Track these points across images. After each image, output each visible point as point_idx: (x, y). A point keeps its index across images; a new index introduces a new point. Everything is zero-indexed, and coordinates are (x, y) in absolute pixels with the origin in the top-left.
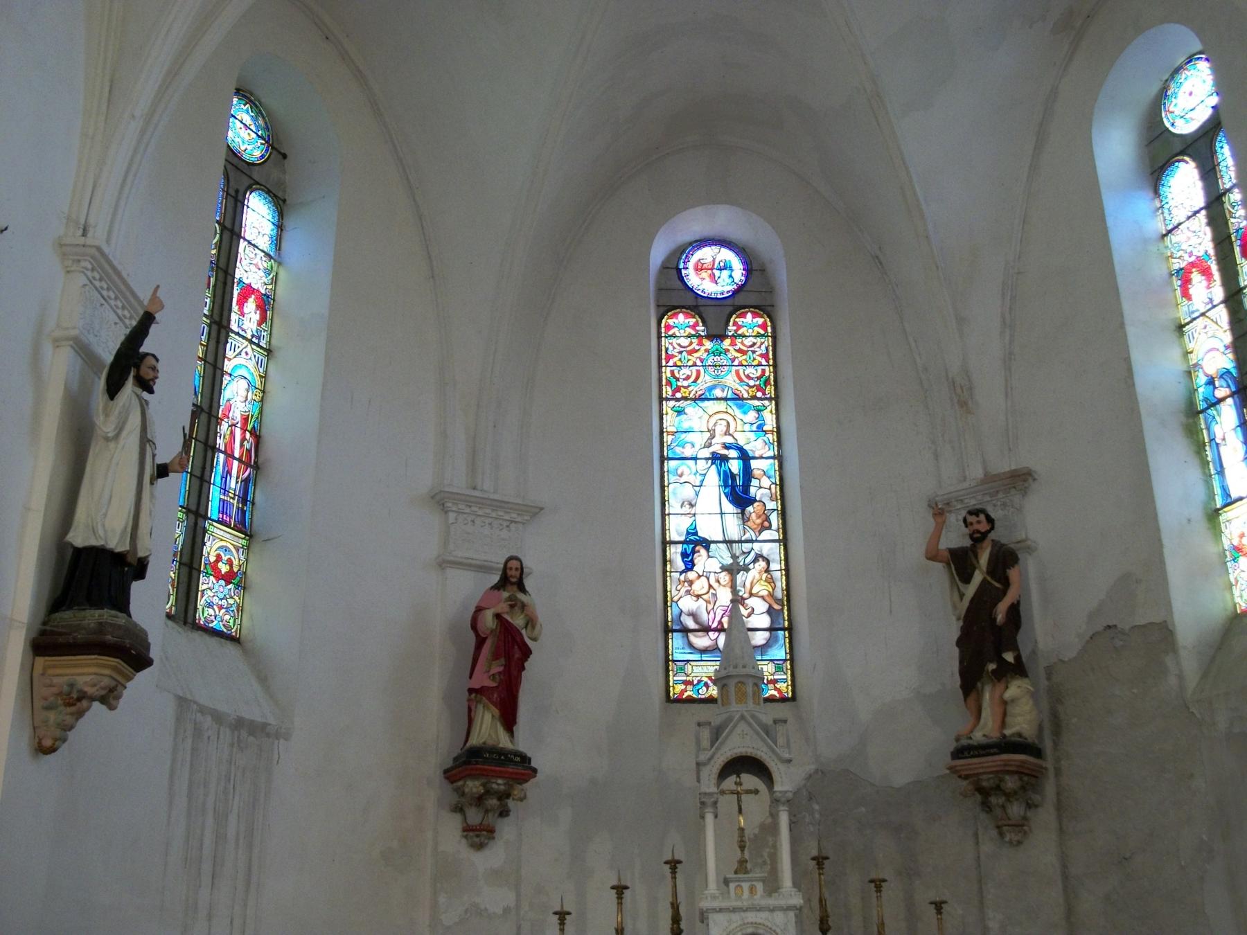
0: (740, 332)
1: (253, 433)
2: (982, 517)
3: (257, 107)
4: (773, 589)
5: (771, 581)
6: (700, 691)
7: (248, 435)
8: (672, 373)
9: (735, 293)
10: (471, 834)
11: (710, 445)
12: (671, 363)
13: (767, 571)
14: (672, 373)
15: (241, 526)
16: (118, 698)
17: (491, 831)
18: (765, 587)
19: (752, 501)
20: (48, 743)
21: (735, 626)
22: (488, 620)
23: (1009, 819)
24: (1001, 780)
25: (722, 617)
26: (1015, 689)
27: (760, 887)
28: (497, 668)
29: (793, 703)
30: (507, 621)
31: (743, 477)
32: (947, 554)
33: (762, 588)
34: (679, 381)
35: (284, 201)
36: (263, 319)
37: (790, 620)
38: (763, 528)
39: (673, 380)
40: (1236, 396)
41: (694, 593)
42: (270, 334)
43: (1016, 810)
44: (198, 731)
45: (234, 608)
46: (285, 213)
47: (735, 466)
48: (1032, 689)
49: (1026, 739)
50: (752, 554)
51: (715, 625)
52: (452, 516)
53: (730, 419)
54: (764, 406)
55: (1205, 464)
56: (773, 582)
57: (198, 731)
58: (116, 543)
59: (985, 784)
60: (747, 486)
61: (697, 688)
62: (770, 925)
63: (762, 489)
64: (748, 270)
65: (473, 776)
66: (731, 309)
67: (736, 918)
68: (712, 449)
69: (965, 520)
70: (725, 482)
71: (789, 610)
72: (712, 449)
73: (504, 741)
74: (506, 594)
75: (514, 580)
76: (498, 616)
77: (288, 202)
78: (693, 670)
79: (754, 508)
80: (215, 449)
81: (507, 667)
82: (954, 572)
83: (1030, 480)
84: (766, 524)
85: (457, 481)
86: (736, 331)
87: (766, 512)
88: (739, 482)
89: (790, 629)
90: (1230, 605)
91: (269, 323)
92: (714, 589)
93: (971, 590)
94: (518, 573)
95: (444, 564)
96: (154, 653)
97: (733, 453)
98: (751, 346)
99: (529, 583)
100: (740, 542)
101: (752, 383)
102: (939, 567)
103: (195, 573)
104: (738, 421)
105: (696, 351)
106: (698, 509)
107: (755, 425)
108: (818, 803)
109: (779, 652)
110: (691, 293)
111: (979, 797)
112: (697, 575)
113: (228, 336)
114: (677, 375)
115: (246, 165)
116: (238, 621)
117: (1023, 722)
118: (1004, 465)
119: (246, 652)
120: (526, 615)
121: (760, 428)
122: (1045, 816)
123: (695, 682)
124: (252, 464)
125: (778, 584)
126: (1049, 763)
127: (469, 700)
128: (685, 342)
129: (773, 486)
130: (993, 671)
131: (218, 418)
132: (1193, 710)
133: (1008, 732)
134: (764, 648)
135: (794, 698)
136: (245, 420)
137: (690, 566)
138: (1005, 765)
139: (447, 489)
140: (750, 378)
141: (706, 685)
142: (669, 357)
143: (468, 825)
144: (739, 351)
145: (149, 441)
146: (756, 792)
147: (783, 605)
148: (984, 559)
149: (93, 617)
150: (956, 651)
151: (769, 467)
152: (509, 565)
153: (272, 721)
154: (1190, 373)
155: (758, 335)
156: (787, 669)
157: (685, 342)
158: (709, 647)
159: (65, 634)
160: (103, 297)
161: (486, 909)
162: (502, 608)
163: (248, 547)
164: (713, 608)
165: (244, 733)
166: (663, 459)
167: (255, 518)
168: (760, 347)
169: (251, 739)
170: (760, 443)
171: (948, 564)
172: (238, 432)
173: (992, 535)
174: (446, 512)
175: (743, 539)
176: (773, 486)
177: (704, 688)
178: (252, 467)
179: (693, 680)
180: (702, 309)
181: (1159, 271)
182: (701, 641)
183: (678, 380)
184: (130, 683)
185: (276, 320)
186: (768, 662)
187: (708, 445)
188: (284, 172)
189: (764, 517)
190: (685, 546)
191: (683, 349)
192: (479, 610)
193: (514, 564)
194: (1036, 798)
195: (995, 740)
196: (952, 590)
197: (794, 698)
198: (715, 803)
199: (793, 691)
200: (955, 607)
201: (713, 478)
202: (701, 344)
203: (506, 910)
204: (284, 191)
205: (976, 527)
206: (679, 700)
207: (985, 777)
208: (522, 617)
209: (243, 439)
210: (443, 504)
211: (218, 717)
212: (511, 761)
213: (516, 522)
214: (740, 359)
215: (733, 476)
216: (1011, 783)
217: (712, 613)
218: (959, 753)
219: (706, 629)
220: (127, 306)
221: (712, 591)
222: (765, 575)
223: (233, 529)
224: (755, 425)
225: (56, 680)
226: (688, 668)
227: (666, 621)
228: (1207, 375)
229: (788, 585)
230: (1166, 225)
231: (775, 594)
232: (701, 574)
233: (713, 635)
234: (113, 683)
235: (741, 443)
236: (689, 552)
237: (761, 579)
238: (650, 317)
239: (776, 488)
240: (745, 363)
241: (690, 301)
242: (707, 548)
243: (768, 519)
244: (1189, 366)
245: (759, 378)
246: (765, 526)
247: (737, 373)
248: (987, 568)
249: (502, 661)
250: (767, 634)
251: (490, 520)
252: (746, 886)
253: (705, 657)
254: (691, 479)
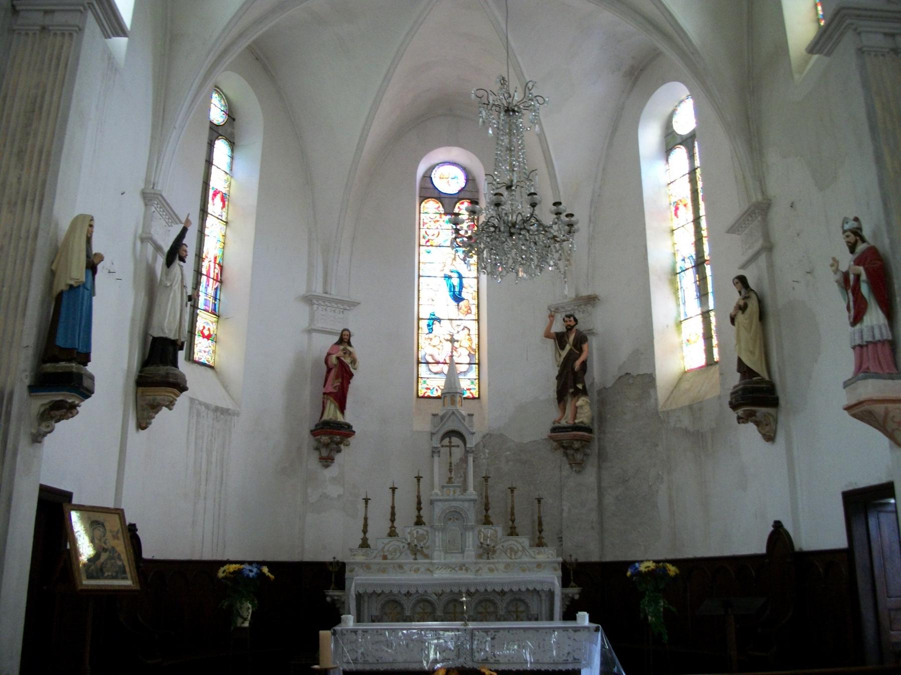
1: (219, 264)
2: (572, 319)
3: (221, 95)
4: (471, 344)
5: (470, 340)
7: (217, 266)
9: (460, 191)
10: (323, 460)
12: (426, 226)
15: (214, 312)
16: (173, 405)
17: (333, 459)
19: (463, 299)
20: (144, 425)
21: (452, 364)
22: (333, 360)
23: (575, 461)
24: (572, 443)
26: (581, 401)
27: (458, 490)
28: (338, 383)
29: (478, 400)
30: (342, 360)
32: (554, 335)
33: (466, 343)
35: (234, 143)
36: (224, 206)
37: (479, 360)
39: (426, 236)
40: (694, 268)
42: (227, 214)
43: (579, 457)
44: (198, 414)
45: (211, 352)
46: (235, 151)
47: (455, 281)
48: (589, 401)
49: (585, 424)
52: (315, 306)
55: (677, 299)
57: (198, 414)
58: (172, 336)
59: (565, 444)
60: (460, 292)
62: (462, 508)
63: (469, 293)
64: (467, 180)
65: (325, 434)
66: (456, 200)
67: (446, 503)
69: (564, 320)
70: (450, 289)
71: (479, 355)
73: (340, 418)
74: (342, 347)
75: (346, 340)
76: (338, 358)
77: (236, 144)
80: (201, 274)
81: (342, 383)
82: (557, 344)
83: (597, 301)
84: (469, 311)
85: (318, 290)
88: (457, 289)
89: (479, 364)
90: (683, 366)
91: (226, 207)
93: (564, 353)
95: (310, 331)
96: (188, 385)
97: (455, 275)
99: (352, 340)
102: (552, 341)
103: (193, 335)
105: (438, 221)
108: (487, 449)
109: (473, 374)
110: (437, 191)
111: (562, 450)
113: (207, 216)
115: (216, 127)
116: (213, 358)
117: (585, 416)
118: (585, 293)
119: (216, 372)
120: (352, 357)
122: (593, 460)
124: (219, 280)
126: (595, 435)
127: (323, 398)
128: (433, 216)
130: (572, 392)
131: (203, 258)
132: (660, 415)
133: (576, 421)
134: (465, 373)
135: (479, 398)
136: (215, 258)
137: (431, 331)
138: (575, 437)
139: (313, 294)
142: (424, 224)
143: (322, 456)
145: (185, 286)
146: (458, 446)
147: (476, 352)
148: (572, 338)
149: (163, 370)
150: (556, 381)
152: (344, 333)
153: (230, 407)
154: (674, 254)
157: (433, 216)
159: (151, 377)
160: (160, 215)
161: (330, 496)
162: (340, 354)
163: (218, 322)
165: (219, 414)
166: (419, 276)
167: (220, 307)
169: (222, 416)
171: (555, 340)
172: (212, 264)
173: (577, 327)
174: (312, 304)
178: (219, 282)
180: (442, 199)
181: (665, 202)
182: (435, 368)
184: (179, 398)
185: (230, 206)
188: (233, 128)
189: (468, 308)
192: (329, 354)
193: (346, 333)
194: (588, 451)
195: (571, 425)
196: (556, 353)
197: (479, 398)
198: (439, 452)
199: (479, 394)
200: (557, 360)
202: (441, 218)
203: (339, 496)
204: (234, 138)
205: (569, 323)
206: (423, 397)
207: (565, 442)
208: (350, 358)
209: (215, 268)
210: (311, 301)
211: (207, 406)
212: (343, 427)
213: (347, 310)
216: (576, 445)
218: (554, 430)
219: (438, 363)
220: (165, 210)
223: (210, 313)
225: (148, 397)
227: (418, 358)
228: (682, 255)
229: (479, 342)
230: (670, 179)
234: (171, 399)
236: (430, 324)
238: (415, 201)
241: (436, 195)
242: (440, 322)
243: (470, 309)
244: (675, 251)
246: (468, 312)
248: (573, 343)
249: (340, 380)
250: (468, 366)
251: (333, 309)
252: (452, 489)
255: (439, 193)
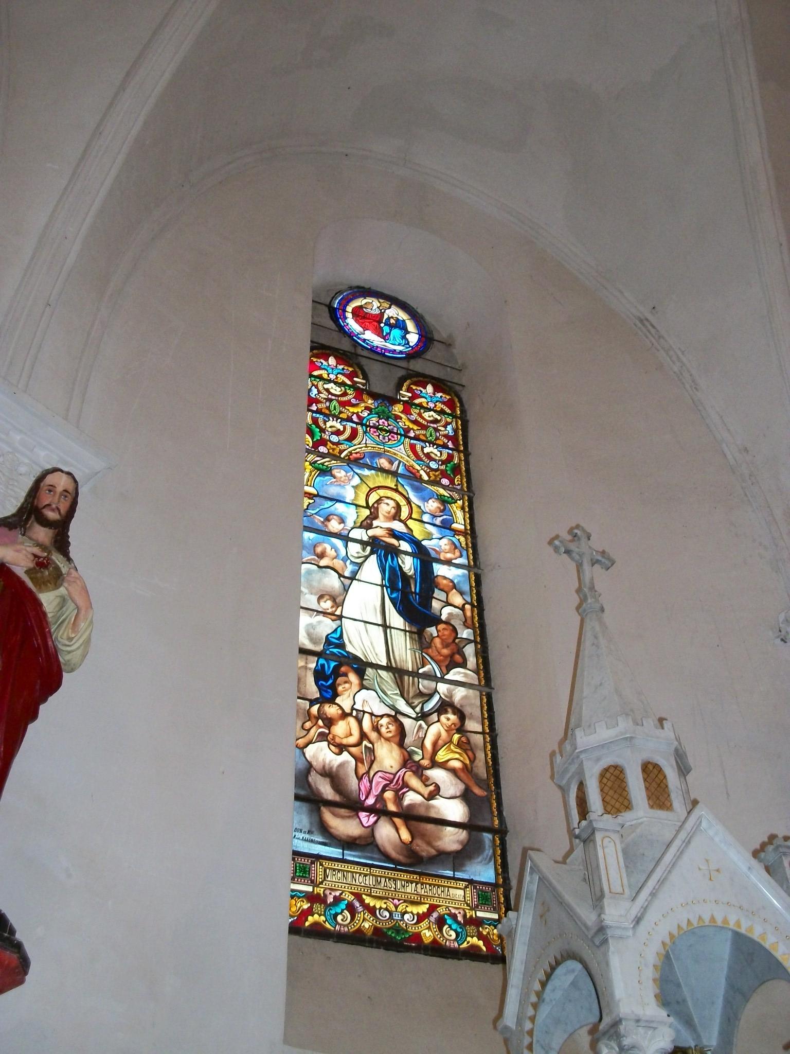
0: (417, 401)
6: (339, 918)
8: (315, 421)
11: (369, 527)
13: (461, 730)
14: (315, 421)
18: (457, 756)
25: (384, 790)
31: (420, 582)
33: (450, 755)
34: (325, 433)
38: (452, 665)
41: (334, 739)
47: (408, 564)
50: (436, 698)
51: (370, 801)
53: (403, 502)
54: (453, 498)
56: (472, 750)
60: (427, 596)
61: (333, 912)
68: (371, 532)
72: (371, 532)
75: (52, 515)
78: (326, 876)
79: (438, 631)
84: (458, 658)
86: (412, 398)
87: (457, 641)
88: (415, 587)
92: (371, 742)
94: (64, 506)
98: (432, 422)
100: (415, 674)
101: (433, 465)
104: (415, 508)
106: (348, 609)
107: (439, 519)
110: (347, 339)
112: (340, 712)
114: (321, 424)
121: (446, 526)
123: (330, 899)
125: (480, 755)
128: (336, 390)
129: (468, 607)
140: (431, 459)
141: (350, 908)
144: (415, 422)
151: (462, 579)
155: (442, 412)
156: (499, 903)
158: (360, 837)
164: (368, 772)
168: (445, 426)
170: (444, 544)
175: (421, 671)
176: (468, 607)
177: (347, 913)
179: (325, 896)
183: (323, 431)
186: (465, 883)
187: (366, 525)
190: (322, 661)
191: (333, 398)
193: (61, 482)
201: (372, 570)
214: (417, 432)
215: (405, 578)
217: (365, 780)
219: (353, 806)
221: (365, 743)
222: (456, 737)
224: (439, 519)
226: (318, 871)
231: (475, 770)
232: (348, 710)
233: (367, 819)
235: (418, 534)
236: (328, 671)
237: (451, 741)
239: (472, 612)
240: (422, 437)
242: (361, 674)
245: (444, 462)
246: (455, 660)
247: (413, 447)
250: (463, 835)
253: (350, 856)
254: (338, 564)
255: (355, 347)
